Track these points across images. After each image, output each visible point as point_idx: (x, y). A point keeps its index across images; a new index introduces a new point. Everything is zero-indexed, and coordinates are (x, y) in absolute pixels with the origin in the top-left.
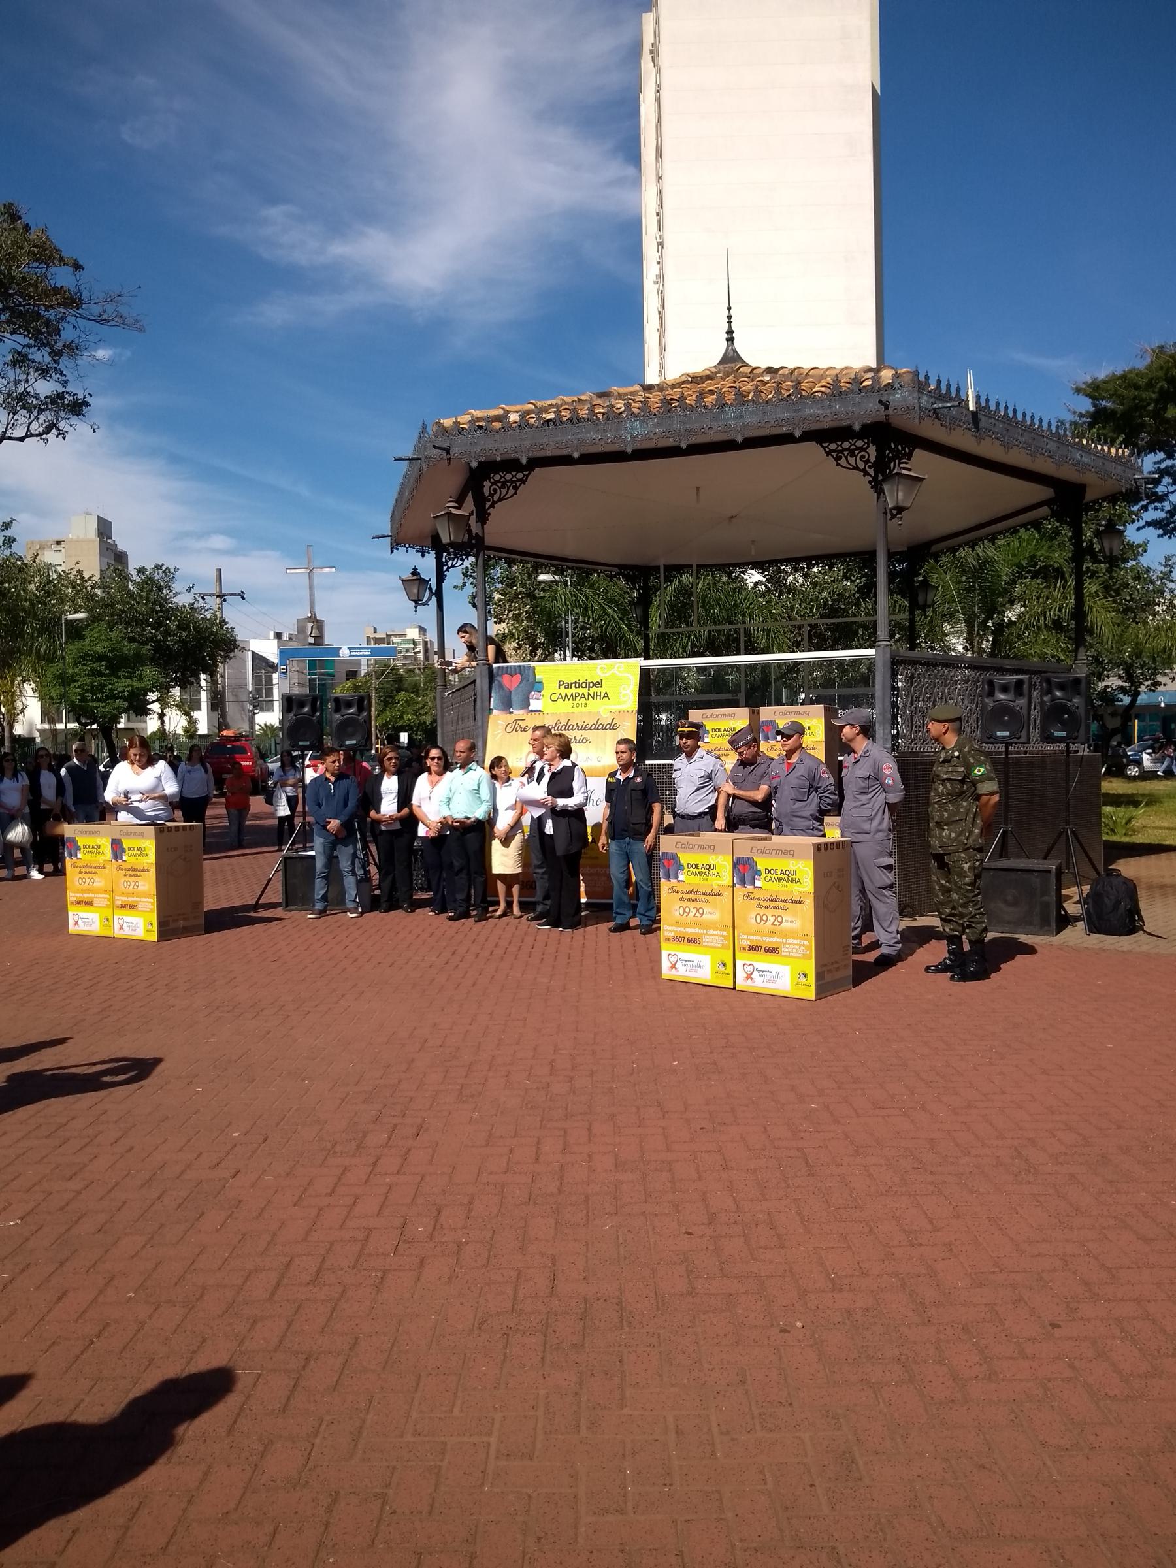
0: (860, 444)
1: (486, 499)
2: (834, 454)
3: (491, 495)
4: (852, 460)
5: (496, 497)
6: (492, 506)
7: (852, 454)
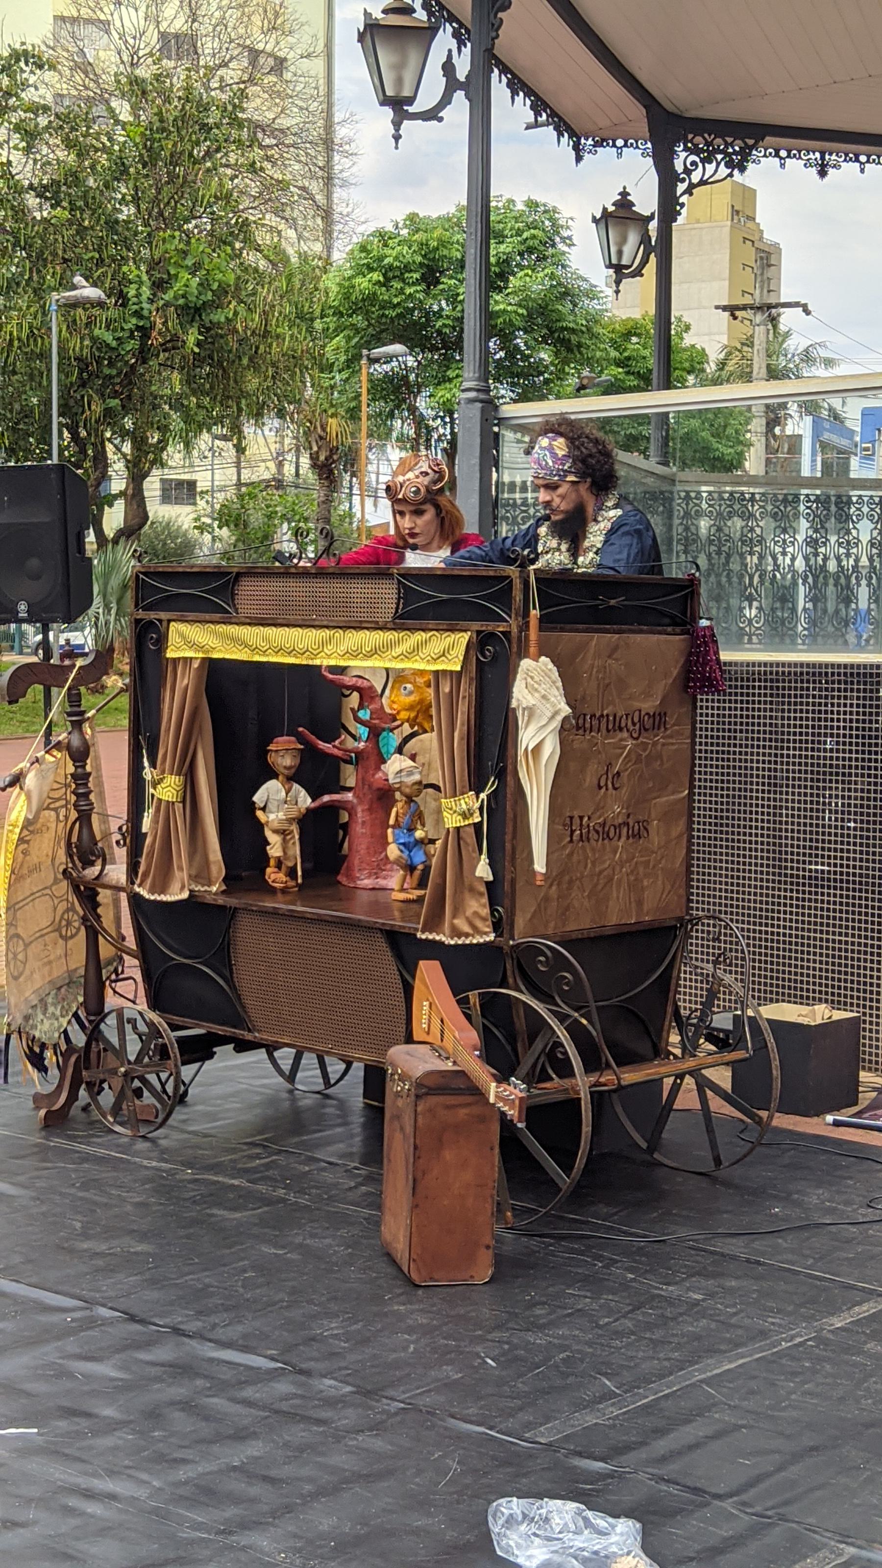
1: (678, 179)
3: (688, 172)
5: (696, 177)
6: (689, 191)
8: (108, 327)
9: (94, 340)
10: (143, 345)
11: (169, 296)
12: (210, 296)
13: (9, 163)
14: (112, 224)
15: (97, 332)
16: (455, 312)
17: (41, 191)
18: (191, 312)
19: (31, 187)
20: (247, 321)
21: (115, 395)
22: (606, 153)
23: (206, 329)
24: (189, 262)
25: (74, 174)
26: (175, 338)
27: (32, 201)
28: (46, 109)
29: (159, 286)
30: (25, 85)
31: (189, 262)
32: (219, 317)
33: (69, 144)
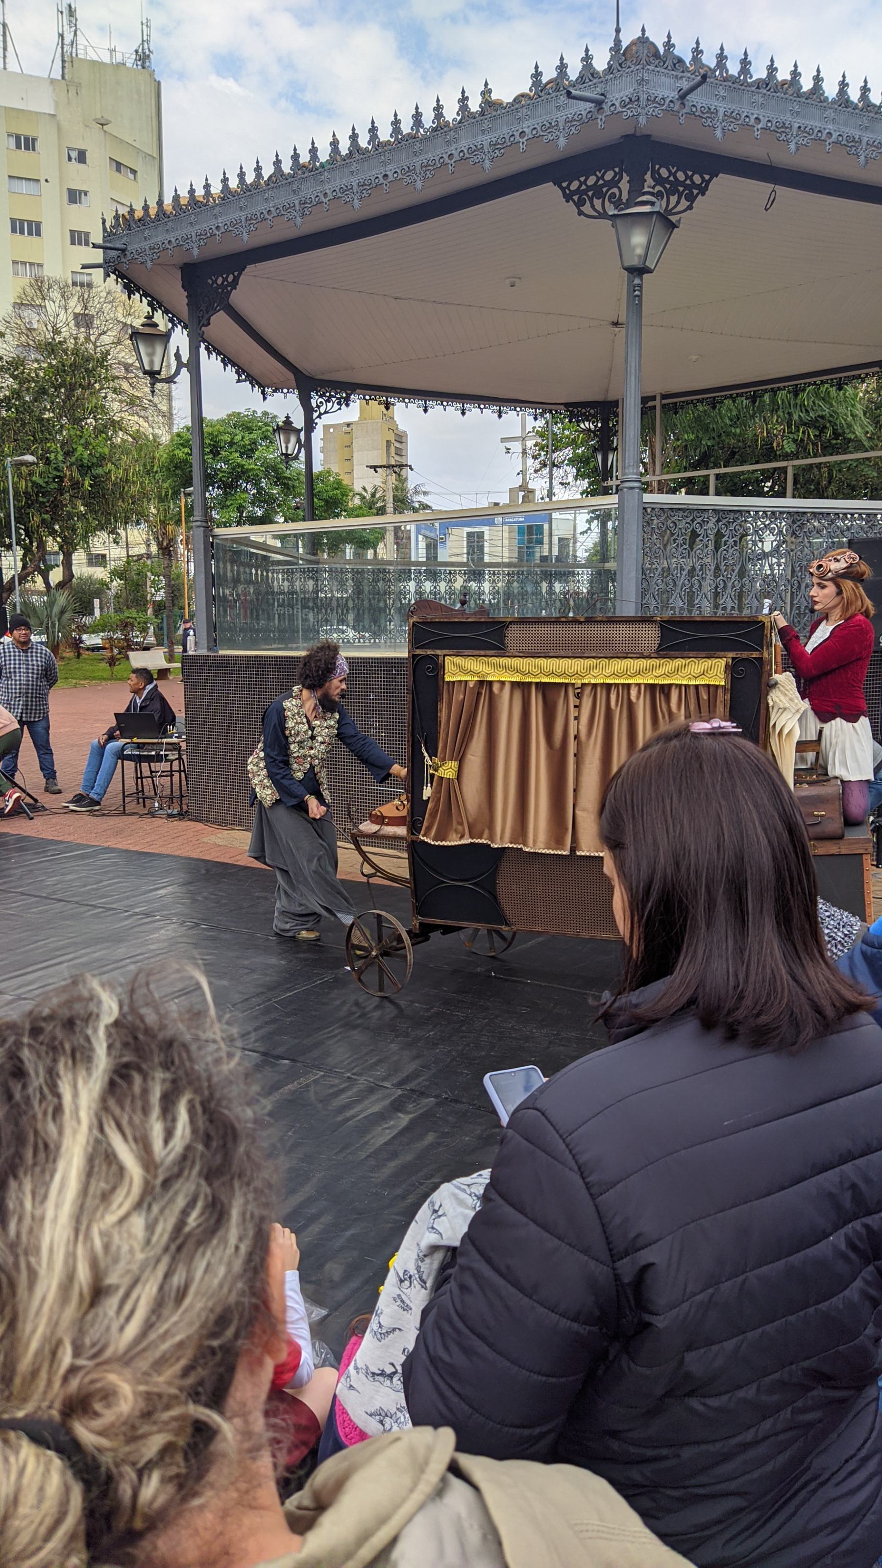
0: (609, 175)
2: (576, 198)
4: (597, 203)
7: (599, 194)
8: (40, 475)
9: (34, 483)
11: (73, 459)
12: (95, 460)
14: (40, 420)
15: (34, 478)
16: (218, 469)
18: (84, 468)
21: (47, 512)
22: (279, 395)
23: (95, 478)
24: (83, 441)
25: (17, 394)
26: (78, 483)
29: (67, 454)
31: (83, 441)
32: (99, 471)
33: (15, 377)
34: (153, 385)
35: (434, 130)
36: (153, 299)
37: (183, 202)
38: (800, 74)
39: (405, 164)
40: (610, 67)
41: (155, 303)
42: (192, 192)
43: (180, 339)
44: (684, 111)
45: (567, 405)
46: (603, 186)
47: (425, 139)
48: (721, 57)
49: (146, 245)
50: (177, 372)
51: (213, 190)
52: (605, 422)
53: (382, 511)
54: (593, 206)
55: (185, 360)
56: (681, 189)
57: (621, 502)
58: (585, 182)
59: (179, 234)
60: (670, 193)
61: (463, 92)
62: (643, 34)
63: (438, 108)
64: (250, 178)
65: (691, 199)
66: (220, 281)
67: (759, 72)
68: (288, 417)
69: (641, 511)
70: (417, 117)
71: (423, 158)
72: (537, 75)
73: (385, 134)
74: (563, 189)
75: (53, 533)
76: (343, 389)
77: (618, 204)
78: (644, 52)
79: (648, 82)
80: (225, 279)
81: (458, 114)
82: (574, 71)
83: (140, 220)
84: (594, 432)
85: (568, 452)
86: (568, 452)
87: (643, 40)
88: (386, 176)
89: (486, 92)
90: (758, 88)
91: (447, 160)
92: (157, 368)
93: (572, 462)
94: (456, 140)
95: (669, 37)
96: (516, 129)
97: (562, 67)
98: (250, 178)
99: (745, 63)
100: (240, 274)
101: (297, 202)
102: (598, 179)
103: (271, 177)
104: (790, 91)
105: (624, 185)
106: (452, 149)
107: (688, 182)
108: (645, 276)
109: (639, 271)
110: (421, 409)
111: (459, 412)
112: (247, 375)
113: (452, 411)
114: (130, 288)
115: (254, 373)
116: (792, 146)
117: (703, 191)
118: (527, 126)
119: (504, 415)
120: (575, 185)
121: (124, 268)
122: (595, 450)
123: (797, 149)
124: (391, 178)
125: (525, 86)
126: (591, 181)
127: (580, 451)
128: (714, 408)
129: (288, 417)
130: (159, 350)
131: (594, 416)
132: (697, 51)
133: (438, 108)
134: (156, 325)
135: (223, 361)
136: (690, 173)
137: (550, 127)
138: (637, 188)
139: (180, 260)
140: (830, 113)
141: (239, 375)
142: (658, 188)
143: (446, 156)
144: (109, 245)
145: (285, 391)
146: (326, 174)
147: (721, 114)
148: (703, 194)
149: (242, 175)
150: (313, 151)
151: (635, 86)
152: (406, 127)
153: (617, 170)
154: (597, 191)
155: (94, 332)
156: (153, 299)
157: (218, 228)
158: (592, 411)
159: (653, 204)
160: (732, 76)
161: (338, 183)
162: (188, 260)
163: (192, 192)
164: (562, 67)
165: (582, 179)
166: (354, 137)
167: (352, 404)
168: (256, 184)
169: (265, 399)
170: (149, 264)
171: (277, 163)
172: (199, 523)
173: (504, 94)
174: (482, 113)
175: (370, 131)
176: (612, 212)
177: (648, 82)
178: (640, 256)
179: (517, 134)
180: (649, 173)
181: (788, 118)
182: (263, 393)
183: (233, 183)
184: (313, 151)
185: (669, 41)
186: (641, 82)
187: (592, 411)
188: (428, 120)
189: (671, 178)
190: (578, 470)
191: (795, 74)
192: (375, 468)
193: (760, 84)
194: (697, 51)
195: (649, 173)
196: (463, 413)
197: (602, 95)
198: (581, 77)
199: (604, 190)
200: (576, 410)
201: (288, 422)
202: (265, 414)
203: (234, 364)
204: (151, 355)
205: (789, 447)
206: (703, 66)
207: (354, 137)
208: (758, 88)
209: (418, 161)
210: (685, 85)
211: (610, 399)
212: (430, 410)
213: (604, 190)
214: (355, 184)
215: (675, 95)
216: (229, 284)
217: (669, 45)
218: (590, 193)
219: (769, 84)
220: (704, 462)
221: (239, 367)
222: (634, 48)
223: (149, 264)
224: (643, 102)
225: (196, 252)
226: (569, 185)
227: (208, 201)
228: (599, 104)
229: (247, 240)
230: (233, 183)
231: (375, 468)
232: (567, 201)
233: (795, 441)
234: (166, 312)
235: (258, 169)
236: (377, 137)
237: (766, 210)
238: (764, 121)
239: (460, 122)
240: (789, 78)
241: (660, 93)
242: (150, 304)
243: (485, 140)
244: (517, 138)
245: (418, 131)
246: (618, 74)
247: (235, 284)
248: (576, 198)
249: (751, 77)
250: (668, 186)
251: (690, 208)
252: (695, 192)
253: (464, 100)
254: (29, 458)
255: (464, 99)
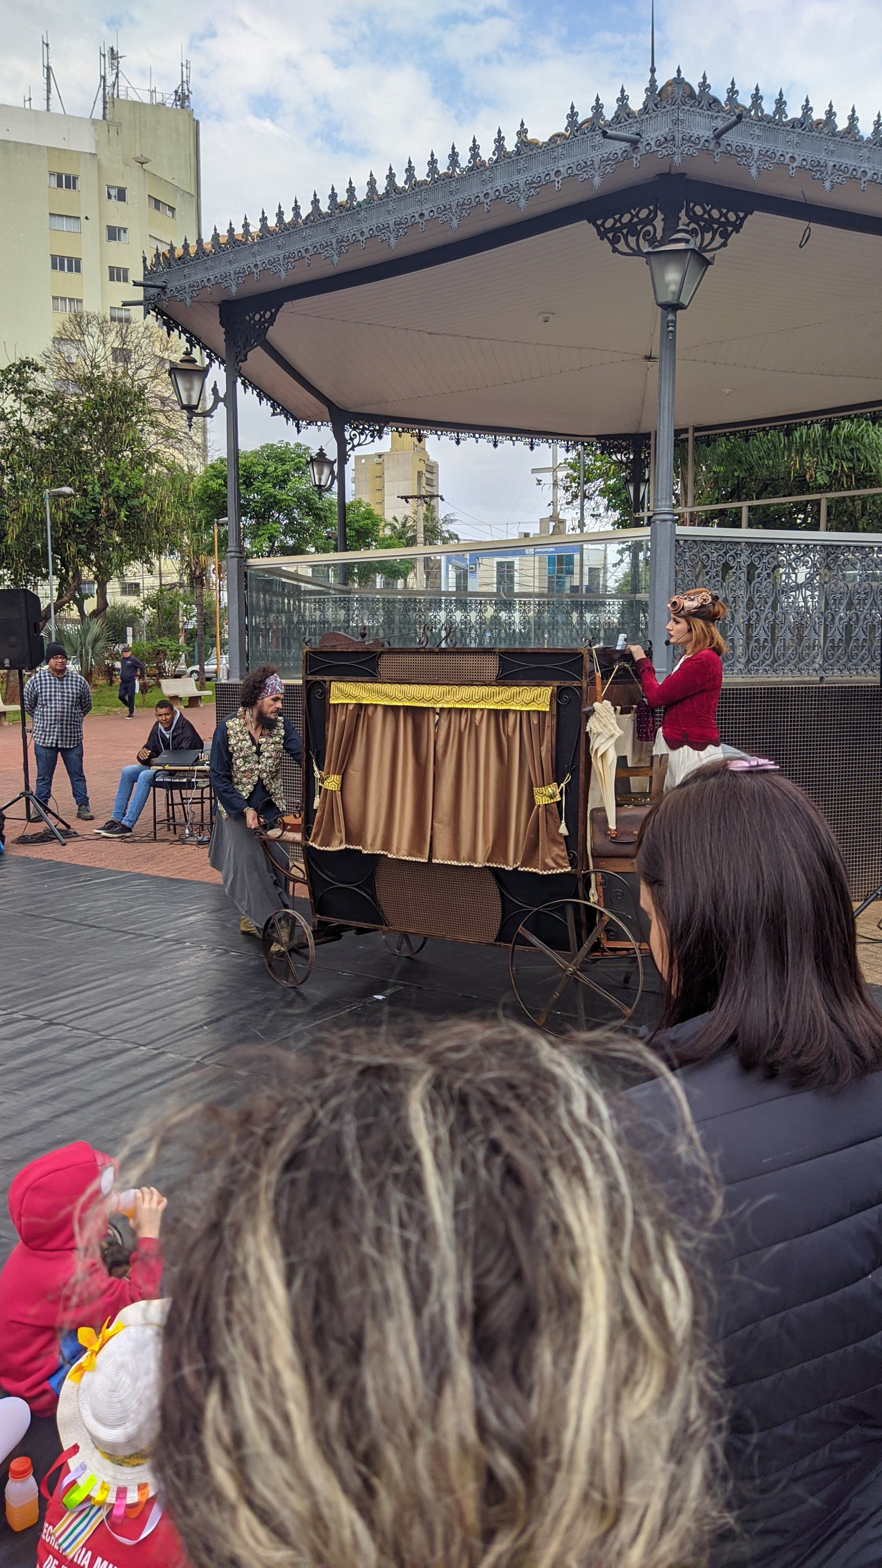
0: (644, 213)
2: (610, 235)
4: (632, 240)
8: (77, 507)
9: (71, 514)
10: (97, 516)
11: (110, 491)
12: (131, 492)
13: (21, 420)
14: (78, 453)
15: (71, 510)
17: (39, 435)
18: (120, 500)
19: (34, 433)
20: (152, 505)
21: (83, 543)
23: (130, 509)
24: (119, 473)
26: (114, 514)
27: (33, 440)
28: (41, 392)
29: (104, 486)
30: (28, 379)
32: (135, 502)
33: (54, 411)
34: (190, 419)
35: (471, 169)
36: (192, 335)
37: (223, 240)
38: (835, 114)
39: (441, 203)
40: (645, 107)
41: (194, 339)
42: (231, 231)
43: (217, 375)
44: (720, 150)
45: (599, 437)
46: (637, 224)
47: (461, 178)
48: (757, 98)
49: (185, 282)
50: (215, 406)
51: (252, 229)
52: (637, 454)
53: (412, 542)
54: (627, 244)
55: (222, 394)
56: (716, 226)
57: (653, 535)
58: (620, 220)
59: (217, 272)
60: (704, 230)
61: (499, 132)
62: (679, 75)
63: (475, 148)
64: (288, 217)
65: (726, 236)
66: (257, 317)
67: (794, 112)
68: (321, 450)
69: (674, 543)
70: (454, 156)
71: (458, 198)
72: (573, 115)
73: (421, 174)
74: (598, 227)
75: (88, 562)
76: (376, 422)
77: (652, 241)
78: (679, 93)
79: (683, 121)
80: (262, 316)
81: (494, 154)
82: (609, 114)
83: (180, 258)
84: (626, 464)
85: (600, 483)
86: (600, 483)
87: (678, 81)
88: (422, 215)
89: (522, 132)
90: (793, 127)
91: (482, 199)
92: (194, 403)
93: (603, 492)
94: (492, 180)
95: (704, 77)
96: (552, 167)
97: (598, 108)
98: (288, 217)
99: (780, 103)
100: (276, 312)
101: (334, 241)
102: (633, 216)
103: (309, 216)
104: (826, 131)
105: (659, 223)
106: (488, 188)
107: (723, 219)
108: (679, 312)
109: (673, 307)
110: (454, 442)
111: (491, 444)
112: (281, 408)
113: (484, 443)
114: (170, 324)
115: (290, 406)
116: (827, 185)
117: (737, 228)
118: (562, 165)
119: (536, 447)
120: (609, 223)
121: (164, 305)
122: (627, 481)
123: (832, 187)
124: (427, 217)
125: (560, 126)
126: (626, 218)
127: (612, 482)
128: (747, 441)
129: (321, 450)
130: (197, 386)
131: (626, 448)
132: (732, 92)
133: (475, 148)
134: (195, 361)
135: (258, 395)
136: (724, 211)
137: (585, 166)
138: (671, 227)
139: (218, 298)
140: (865, 152)
141: (274, 409)
142: (693, 226)
143: (481, 195)
144: (149, 283)
145: (319, 423)
146: (363, 213)
147: (756, 153)
148: (738, 232)
149: (280, 214)
150: (351, 190)
151: (670, 126)
152: (443, 167)
153: (652, 208)
154: (632, 230)
155: (132, 366)
156: (192, 335)
157: (256, 266)
158: (624, 444)
159: (687, 241)
160: (767, 116)
161: (374, 222)
162: (225, 298)
163: (231, 231)
164: (598, 108)
165: (617, 217)
166: (391, 177)
167: (384, 436)
168: (294, 223)
169: (299, 431)
170: (188, 302)
171: (315, 202)
172: (233, 554)
173: (540, 134)
174: (518, 152)
175: (407, 170)
176: (646, 249)
177: (683, 121)
178: (674, 293)
179: (552, 173)
180: (684, 211)
181: (822, 157)
182: (297, 426)
183: (272, 222)
184: (351, 190)
185: (705, 81)
186: (677, 122)
187: (624, 444)
188: (464, 160)
189: (706, 216)
190: (610, 501)
191: (830, 113)
192: (406, 498)
193: (795, 124)
194: (732, 92)
195: (684, 211)
196: (495, 445)
197: (638, 134)
198: (617, 116)
199: (639, 227)
200: (609, 443)
201: (321, 454)
202: (298, 445)
203: (269, 398)
204: (189, 390)
205: (823, 479)
206: (738, 106)
207: (391, 177)
208: (793, 127)
209: (454, 200)
210: (720, 125)
211: (642, 431)
212: (462, 442)
213: (639, 227)
214: (391, 223)
215: (710, 134)
216: (266, 321)
217: (704, 85)
218: (625, 231)
219: (804, 123)
220: (735, 494)
221: (274, 401)
222: (670, 88)
223: (188, 302)
224: (678, 141)
225: (234, 289)
226: (603, 223)
227: (247, 240)
228: (634, 143)
229: (284, 277)
230: (272, 222)
231: (406, 498)
232: (602, 239)
233: (828, 473)
234: (204, 347)
235: (296, 208)
236: (414, 176)
237: (801, 247)
238: (799, 159)
239: (496, 162)
240: (824, 117)
241: (695, 132)
242: (188, 340)
243: (520, 179)
244: (553, 177)
245: (454, 171)
246: (653, 115)
247: (272, 320)
248: (610, 235)
249: (786, 117)
250: (702, 224)
251: (724, 245)
252: (730, 229)
253: (500, 140)
254: (67, 490)
255: (500, 140)
